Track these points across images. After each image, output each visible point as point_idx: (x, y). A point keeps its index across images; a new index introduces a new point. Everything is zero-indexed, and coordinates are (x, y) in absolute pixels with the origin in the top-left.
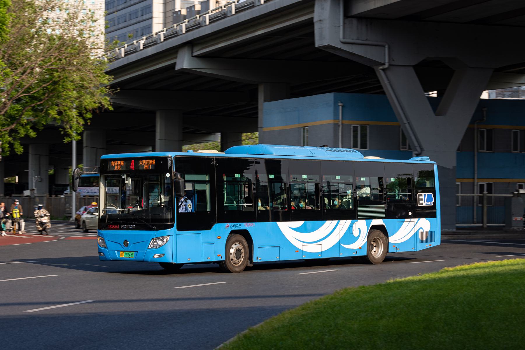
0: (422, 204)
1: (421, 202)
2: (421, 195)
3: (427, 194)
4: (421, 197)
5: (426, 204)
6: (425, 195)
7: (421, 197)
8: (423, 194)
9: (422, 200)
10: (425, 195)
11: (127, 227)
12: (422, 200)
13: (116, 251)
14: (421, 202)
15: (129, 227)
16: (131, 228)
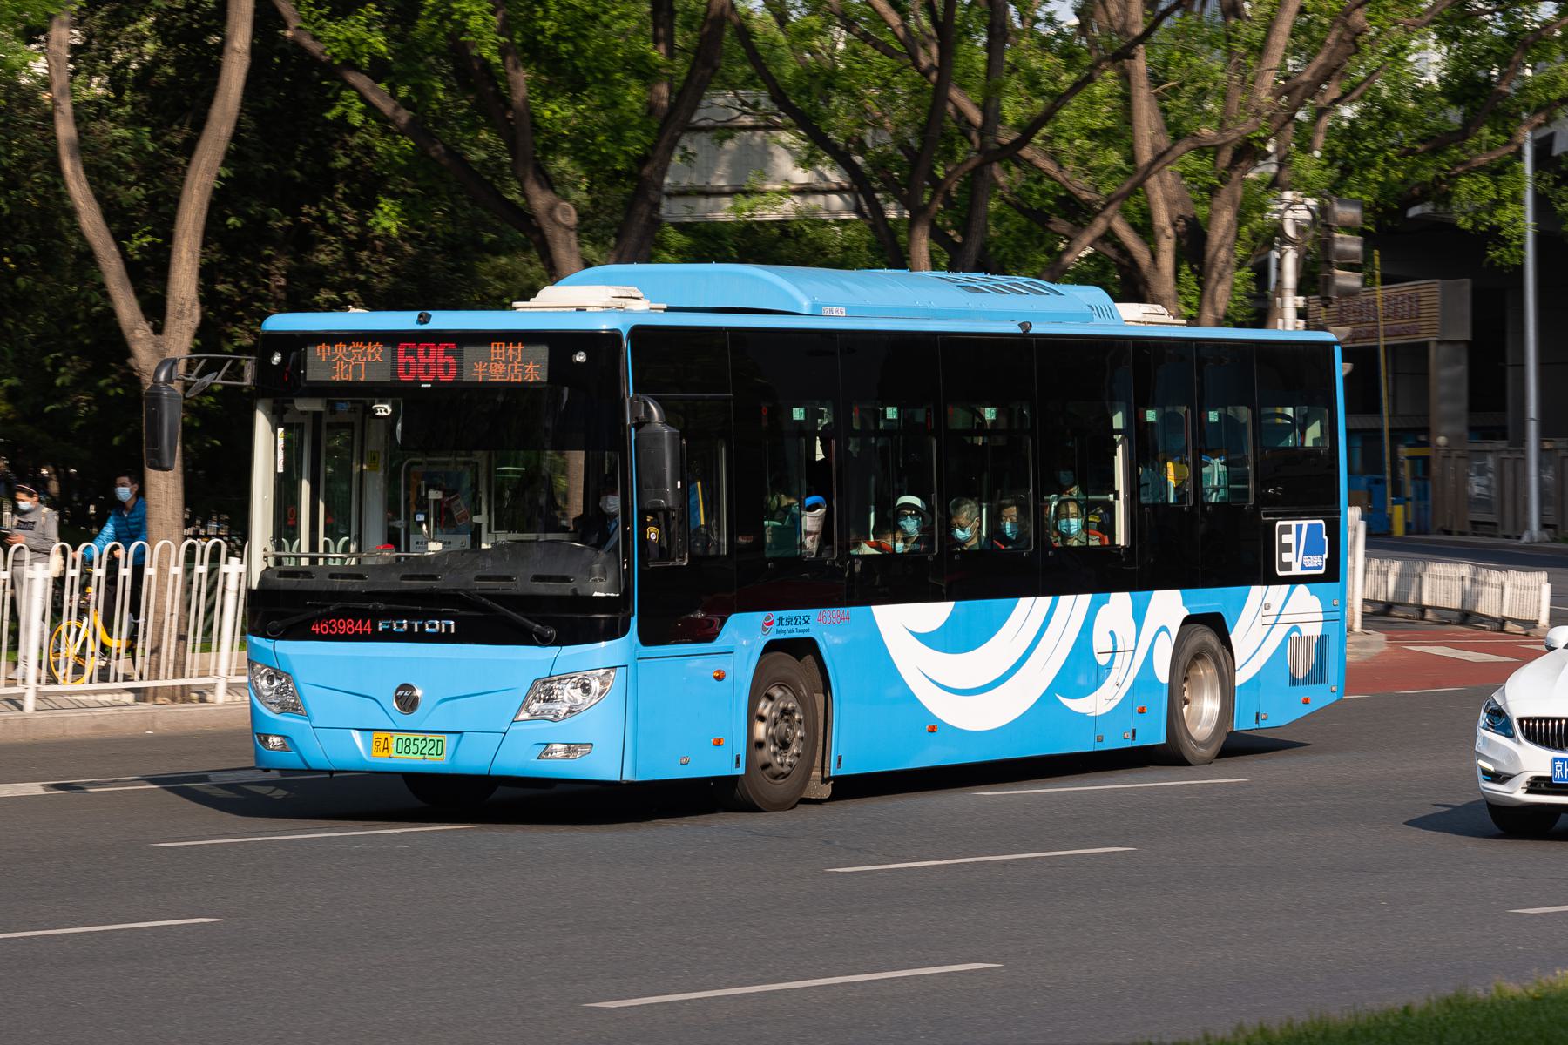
0: (1288, 566)
1: (1286, 557)
2: (1287, 530)
3: (1305, 523)
4: (1286, 539)
5: (1303, 568)
6: (1299, 528)
7: (1286, 539)
8: (1294, 523)
9: (1288, 548)
10: (1299, 528)
11: (411, 627)
12: (1288, 548)
13: (356, 735)
14: (1286, 557)
15: (422, 627)
16: (433, 630)
